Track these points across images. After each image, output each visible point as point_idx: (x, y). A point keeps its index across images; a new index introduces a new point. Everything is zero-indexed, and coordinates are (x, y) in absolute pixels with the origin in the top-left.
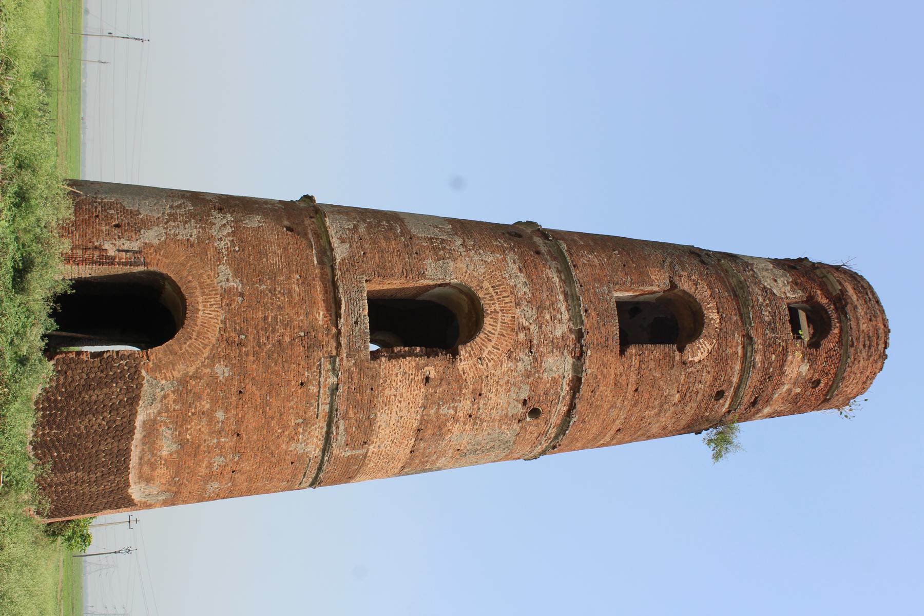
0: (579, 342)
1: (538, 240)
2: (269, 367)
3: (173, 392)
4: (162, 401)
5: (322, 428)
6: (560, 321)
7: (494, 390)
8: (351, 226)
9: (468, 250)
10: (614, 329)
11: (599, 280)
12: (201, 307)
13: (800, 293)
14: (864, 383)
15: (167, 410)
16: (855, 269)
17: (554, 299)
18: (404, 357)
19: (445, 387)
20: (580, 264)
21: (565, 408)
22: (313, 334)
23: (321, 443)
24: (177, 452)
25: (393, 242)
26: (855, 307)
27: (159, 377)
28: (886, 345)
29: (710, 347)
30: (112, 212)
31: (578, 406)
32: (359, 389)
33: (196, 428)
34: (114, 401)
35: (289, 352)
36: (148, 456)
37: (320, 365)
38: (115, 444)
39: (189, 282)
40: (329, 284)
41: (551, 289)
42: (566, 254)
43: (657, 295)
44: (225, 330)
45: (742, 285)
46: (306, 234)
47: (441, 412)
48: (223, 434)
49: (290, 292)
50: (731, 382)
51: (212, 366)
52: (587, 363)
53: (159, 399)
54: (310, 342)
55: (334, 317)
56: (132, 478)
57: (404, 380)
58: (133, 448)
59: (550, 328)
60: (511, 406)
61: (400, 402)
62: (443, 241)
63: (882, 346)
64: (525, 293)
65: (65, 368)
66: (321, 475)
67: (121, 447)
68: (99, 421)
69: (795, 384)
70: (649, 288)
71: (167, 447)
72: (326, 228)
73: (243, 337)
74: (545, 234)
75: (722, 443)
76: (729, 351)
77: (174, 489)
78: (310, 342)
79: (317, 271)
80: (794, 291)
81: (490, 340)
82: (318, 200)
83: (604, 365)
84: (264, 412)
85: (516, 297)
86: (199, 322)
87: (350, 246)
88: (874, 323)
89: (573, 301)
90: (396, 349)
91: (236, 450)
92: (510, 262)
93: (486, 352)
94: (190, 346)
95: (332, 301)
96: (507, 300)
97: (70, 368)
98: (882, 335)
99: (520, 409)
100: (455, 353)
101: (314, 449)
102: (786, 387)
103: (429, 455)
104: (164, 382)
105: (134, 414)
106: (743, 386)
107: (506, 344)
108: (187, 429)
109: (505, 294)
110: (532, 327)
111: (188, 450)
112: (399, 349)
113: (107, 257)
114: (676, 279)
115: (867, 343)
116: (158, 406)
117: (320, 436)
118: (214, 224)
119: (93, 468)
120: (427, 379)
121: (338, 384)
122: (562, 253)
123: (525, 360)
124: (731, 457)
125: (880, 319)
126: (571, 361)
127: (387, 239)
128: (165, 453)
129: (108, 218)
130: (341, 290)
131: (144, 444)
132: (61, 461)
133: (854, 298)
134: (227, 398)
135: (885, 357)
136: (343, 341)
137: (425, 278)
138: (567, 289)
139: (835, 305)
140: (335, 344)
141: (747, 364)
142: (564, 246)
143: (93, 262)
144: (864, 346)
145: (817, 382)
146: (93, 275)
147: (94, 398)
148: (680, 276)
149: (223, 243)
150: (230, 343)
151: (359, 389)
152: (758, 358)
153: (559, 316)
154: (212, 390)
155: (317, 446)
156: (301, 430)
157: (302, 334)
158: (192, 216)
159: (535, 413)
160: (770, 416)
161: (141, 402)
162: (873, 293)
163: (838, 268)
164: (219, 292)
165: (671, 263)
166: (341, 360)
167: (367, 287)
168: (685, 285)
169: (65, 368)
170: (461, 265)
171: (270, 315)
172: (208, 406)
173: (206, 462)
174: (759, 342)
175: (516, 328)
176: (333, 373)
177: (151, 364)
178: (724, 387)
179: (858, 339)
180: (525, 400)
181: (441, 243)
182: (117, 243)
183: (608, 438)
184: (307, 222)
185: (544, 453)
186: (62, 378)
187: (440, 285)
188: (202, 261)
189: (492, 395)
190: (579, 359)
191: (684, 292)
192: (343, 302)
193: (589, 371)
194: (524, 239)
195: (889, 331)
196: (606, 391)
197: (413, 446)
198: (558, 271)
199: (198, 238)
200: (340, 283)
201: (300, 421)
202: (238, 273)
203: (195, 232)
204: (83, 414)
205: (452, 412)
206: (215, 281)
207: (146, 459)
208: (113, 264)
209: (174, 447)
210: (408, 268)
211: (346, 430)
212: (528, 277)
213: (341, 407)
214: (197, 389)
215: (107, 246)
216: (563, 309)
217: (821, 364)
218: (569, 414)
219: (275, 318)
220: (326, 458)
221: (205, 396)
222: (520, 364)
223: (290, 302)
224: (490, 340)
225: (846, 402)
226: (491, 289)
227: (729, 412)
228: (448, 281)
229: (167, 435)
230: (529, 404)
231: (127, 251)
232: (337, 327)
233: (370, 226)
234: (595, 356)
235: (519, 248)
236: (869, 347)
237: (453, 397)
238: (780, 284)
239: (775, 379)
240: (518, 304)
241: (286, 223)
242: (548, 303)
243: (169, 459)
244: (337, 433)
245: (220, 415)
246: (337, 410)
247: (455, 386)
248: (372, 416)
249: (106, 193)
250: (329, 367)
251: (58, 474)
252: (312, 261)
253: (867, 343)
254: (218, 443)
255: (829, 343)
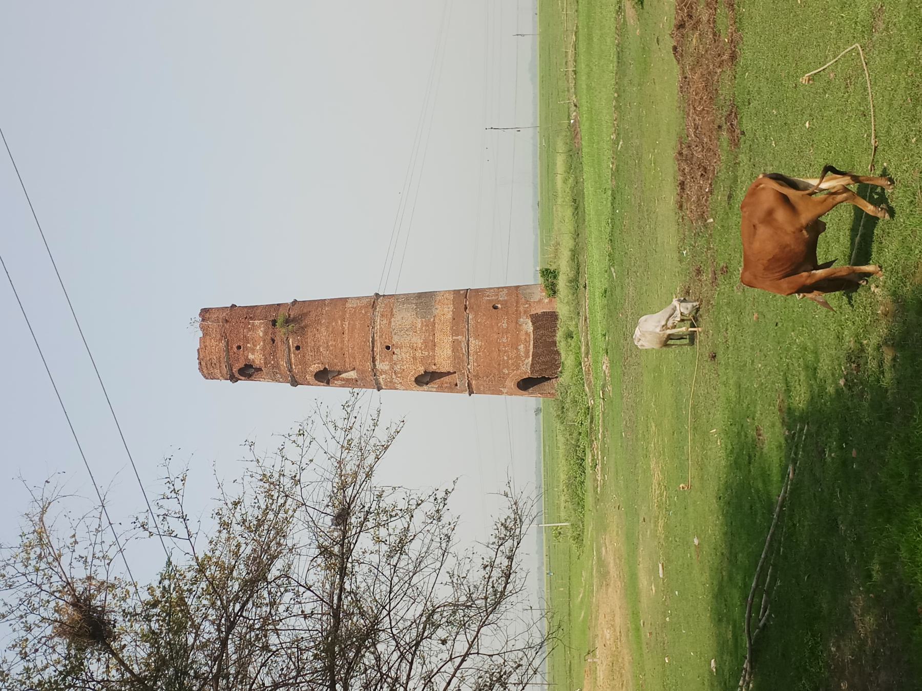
27: (526, 369)
28: (200, 363)
32: (459, 363)
33: (513, 354)
54: (477, 377)
71: (521, 347)
78: (477, 377)
100: (425, 372)
111: (515, 347)
123: (397, 368)
141: (289, 362)
145: (239, 347)
159: (388, 348)
213: (465, 357)
218: (373, 347)
237: (423, 359)
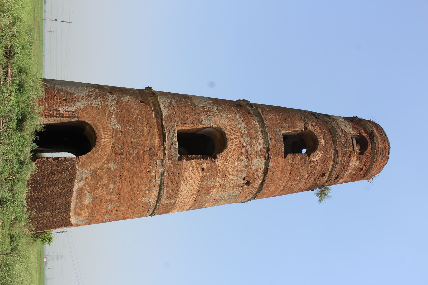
0: (268, 152)
1: (248, 107)
2: (133, 164)
3: (91, 176)
4: (85, 180)
5: (157, 191)
6: (260, 143)
7: (231, 174)
8: (169, 101)
9: (220, 112)
10: (282, 147)
11: (275, 126)
12: (103, 137)
13: (356, 132)
14: (380, 169)
15: (88, 184)
16: (375, 121)
17: (257, 134)
18: (193, 160)
19: (210, 172)
20: (267, 119)
21: (261, 181)
22: (153, 149)
23: (156, 198)
24: (92, 203)
25: (188, 108)
26: (377, 138)
29: (320, 155)
30: (62, 93)
31: (266, 180)
32: (173, 174)
33: (101, 192)
34: (64, 180)
35: (143, 157)
36: (79, 204)
37: (156, 163)
38: (64, 199)
39: (98, 125)
40: (160, 127)
41: (256, 130)
42: (262, 114)
43: (299, 132)
44: (114, 147)
45: (333, 128)
46: (149, 104)
47: (209, 183)
48: (113, 194)
49: (143, 130)
50: (328, 169)
51: (108, 164)
52: (271, 162)
53: (84, 179)
54: (152, 153)
55: (162, 142)
56: (72, 214)
57: (193, 170)
58: (72, 201)
59: (255, 146)
60: (238, 181)
61: (191, 179)
62: (209, 108)
63: (387, 154)
64: (245, 131)
65: (41, 165)
66: (155, 211)
67: (67, 200)
68: (57, 189)
69: (353, 170)
70: (296, 129)
71: (87, 200)
72: (158, 102)
73: (122, 151)
74: (251, 105)
75: (322, 195)
76: (328, 156)
77: (90, 218)
78: (152, 153)
79: (155, 121)
80: (353, 131)
81: (230, 152)
82: (154, 89)
83: (278, 162)
84: (131, 184)
85: (241, 133)
86: (102, 144)
87: (169, 110)
88: (384, 144)
89: (265, 134)
90: (189, 156)
91: (118, 201)
92: (238, 117)
93: (228, 157)
94: (98, 155)
95: (161, 134)
96: (237, 134)
97: (43, 165)
98: (387, 149)
99: (242, 182)
100: (215, 158)
101: (152, 200)
102: (350, 171)
103: (202, 202)
104: (86, 171)
105: (73, 186)
106: (333, 171)
107: (237, 154)
108: (97, 192)
109: (236, 132)
110: (248, 146)
111: (97, 201)
112: (190, 156)
113: (60, 114)
114: (307, 125)
115: (382, 153)
116: (83, 182)
117: (156, 195)
118: (108, 99)
119: (54, 210)
120: (203, 169)
121: (164, 172)
122: (260, 114)
124: (327, 201)
125: (387, 143)
126: (264, 161)
127: (185, 107)
128: (87, 203)
129: (60, 96)
130: (165, 130)
131: (77, 199)
132: (39, 207)
133: (377, 134)
134: (115, 178)
135: (388, 158)
136: (167, 152)
137: (202, 124)
138: (262, 129)
139: (369, 136)
140: (163, 154)
142: (260, 111)
143: (54, 116)
144: (381, 154)
145: (362, 169)
146: (54, 122)
147: (54, 179)
148: (308, 124)
149: (112, 108)
150: (116, 153)
151: (173, 174)
152: (340, 159)
153: (259, 141)
154: (108, 175)
155: (154, 199)
156: (147, 192)
157: (148, 149)
158: (98, 95)
159: (248, 183)
160: (342, 183)
161: (76, 180)
162: (384, 132)
163: (369, 121)
164: (111, 130)
165: (304, 118)
166: (166, 161)
167: (177, 128)
168: (310, 128)
169: (41, 165)
170: (217, 119)
171: (134, 141)
172: (106, 182)
173: (105, 207)
174: (340, 152)
175: (241, 146)
176: (162, 167)
177: (80, 163)
178: (325, 172)
179: (378, 151)
180: (244, 178)
181: (208, 109)
182: (65, 108)
183: (277, 194)
184: (150, 99)
185: (250, 200)
186: (40, 170)
187: (208, 128)
188: (103, 116)
189: (230, 176)
190: (267, 160)
191: (310, 131)
192: (166, 135)
193: (271, 165)
194: (242, 106)
195: (390, 148)
196: (278, 173)
197: (196, 198)
198: (258, 122)
199: (101, 105)
200: (165, 126)
201: (147, 188)
202: (119, 121)
203: (100, 103)
204: (50, 186)
205: (213, 183)
206: (109, 125)
207: (78, 206)
208: (63, 117)
209: (91, 200)
210: (195, 120)
211: (167, 192)
212: (246, 124)
213: (165, 181)
214: (101, 175)
215: (60, 109)
216: (261, 138)
217: (364, 161)
218: (262, 184)
219: (136, 142)
220: (158, 204)
221: (105, 177)
222: (242, 162)
223: (143, 135)
224: (230, 152)
225: (371, 177)
226: (230, 129)
227: (327, 182)
228: (212, 126)
229: (88, 195)
230: (246, 179)
231: (69, 111)
232: (164, 146)
233: (177, 102)
234: (274, 158)
235: (242, 111)
236: (383, 154)
237: (214, 177)
238: (348, 128)
239: (346, 167)
240: (242, 136)
241: (140, 99)
242: (254, 136)
243: (88, 205)
244: (163, 193)
245: (111, 186)
246: (163, 183)
247: (215, 172)
248: (179, 186)
249: (59, 85)
250: (160, 164)
251: (38, 213)
252: (152, 116)
253: (382, 153)
254: (110, 198)
255: (367, 153)
